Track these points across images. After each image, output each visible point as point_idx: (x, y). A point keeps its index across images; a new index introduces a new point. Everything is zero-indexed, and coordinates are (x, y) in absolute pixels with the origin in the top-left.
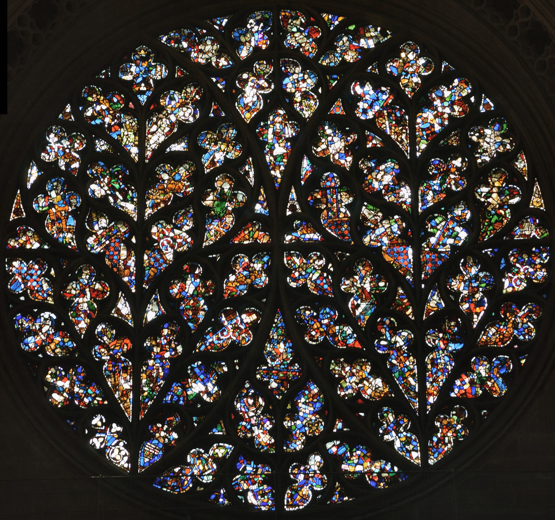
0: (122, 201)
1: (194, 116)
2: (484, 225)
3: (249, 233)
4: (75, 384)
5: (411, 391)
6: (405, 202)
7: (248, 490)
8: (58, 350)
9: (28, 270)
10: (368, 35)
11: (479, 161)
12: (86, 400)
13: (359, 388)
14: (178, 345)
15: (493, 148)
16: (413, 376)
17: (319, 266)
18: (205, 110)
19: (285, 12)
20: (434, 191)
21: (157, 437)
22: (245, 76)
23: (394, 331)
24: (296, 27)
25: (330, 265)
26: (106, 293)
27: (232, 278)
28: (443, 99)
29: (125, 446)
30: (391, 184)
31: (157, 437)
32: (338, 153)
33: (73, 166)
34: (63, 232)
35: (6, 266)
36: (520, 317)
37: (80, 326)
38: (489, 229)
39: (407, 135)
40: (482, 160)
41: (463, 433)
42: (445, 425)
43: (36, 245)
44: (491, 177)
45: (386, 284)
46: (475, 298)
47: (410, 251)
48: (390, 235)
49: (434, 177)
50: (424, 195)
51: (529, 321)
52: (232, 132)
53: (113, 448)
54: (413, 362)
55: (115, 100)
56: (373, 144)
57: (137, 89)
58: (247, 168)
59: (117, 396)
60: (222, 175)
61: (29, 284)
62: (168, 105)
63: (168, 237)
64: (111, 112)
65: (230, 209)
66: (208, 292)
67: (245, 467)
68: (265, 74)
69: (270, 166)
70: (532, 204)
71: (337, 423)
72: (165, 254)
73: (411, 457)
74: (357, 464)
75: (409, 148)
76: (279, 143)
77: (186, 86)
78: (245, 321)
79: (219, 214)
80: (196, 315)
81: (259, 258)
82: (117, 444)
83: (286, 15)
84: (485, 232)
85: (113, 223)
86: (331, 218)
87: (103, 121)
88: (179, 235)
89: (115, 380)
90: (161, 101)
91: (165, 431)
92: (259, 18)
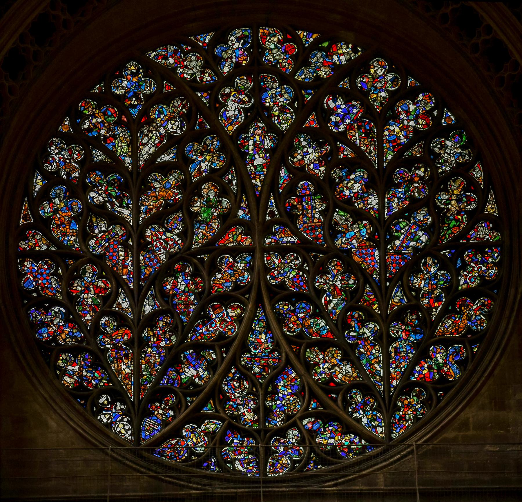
0: (118, 207)
1: (181, 129)
2: (443, 229)
3: (233, 236)
4: (83, 368)
5: (377, 375)
6: (373, 209)
7: (235, 459)
8: (68, 340)
9: (38, 270)
10: (340, 52)
11: (440, 170)
12: (94, 382)
13: (332, 373)
14: (172, 335)
15: (453, 159)
16: (379, 363)
17: (295, 266)
19: (263, 29)
20: (399, 198)
21: (156, 414)
22: (227, 91)
23: (362, 323)
24: (274, 44)
26: (108, 289)
28: (408, 113)
30: (361, 192)
31: (156, 414)
32: (313, 163)
34: (67, 236)
35: (19, 266)
36: (473, 310)
37: (86, 318)
38: (448, 233)
39: (375, 147)
40: (443, 170)
41: (422, 411)
42: (406, 404)
43: (45, 247)
44: (451, 185)
45: (355, 282)
46: (434, 294)
47: (377, 253)
48: (359, 239)
49: (399, 186)
50: (390, 202)
51: (481, 314)
53: (119, 423)
54: (379, 351)
55: (109, 113)
56: (344, 154)
57: (129, 102)
58: (230, 176)
60: (208, 183)
61: (40, 282)
62: (158, 118)
63: (160, 239)
64: (106, 125)
65: (215, 214)
66: (198, 289)
67: (233, 440)
68: (245, 89)
69: (250, 175)
70: (487, 211)
71: (312, 403)
72: (158, 255)
73: (376, 432)
74: (330, 438)
75: (377, 159)
76: (259, 154)
77: (173, 99)
78: (230, 315)
79: (206, 219)
80: (188, 309)
81: (242, 258)
82: (122, 420)
83: (264, 32)
84: (444, 235)
85: (112, 227)
86: (306, 223)
87: (99, 133)
88: (170, 238)
89: (118, 365)
90: (151, 114)
91: (162, 409)
92: (239, 35)
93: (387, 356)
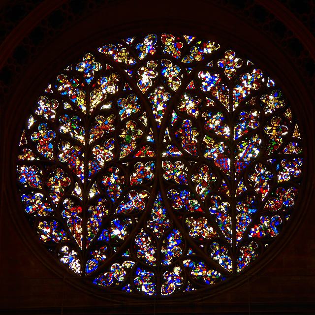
1: (115, 90)
3: (144, 151)
6: (226, 135)
7: (142, 285)
8: (44, 213)
10: (208, 46)
11: (266, 113)
12: (59, 239)
16: (229, 226)
17: (180, 169)
20: (242, 129)
22: (142, 69)
23: (220, 203)
25: (186, 168)
27: (135, 175)
28: (247, 80)
29: (78, 262)
33: (52, 117)
43: (33, 159)
47: (229, 161)
49: (242, 121)
50: (237, 131)
52: (136, 99)
55: (74, 82)
58: (143, 117)
59: (74, 236)
61: (29, 179)
63: (101, 153)
65: (134, 139)
73: (227, 268)
74: (199, 272)
77: (111, 74)
78: (141, 197)
82: (75, 261)
84: (270, 149)
91: (99, 255)
93: (234, 221)
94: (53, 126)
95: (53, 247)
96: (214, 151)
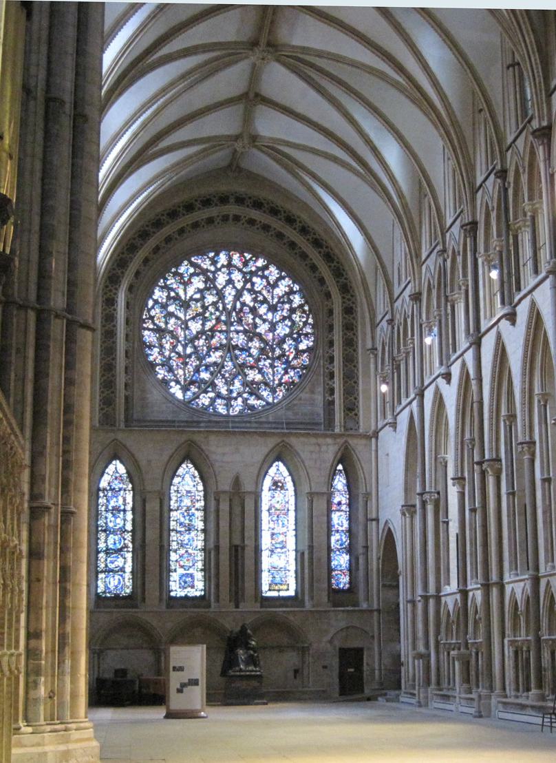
18: (206, 284)
23: (265, 360)
28: (282, 284)
47: (271, 335)
52: (215, 292)
93: (274, 373)
94: (164, 306)
95: (165, 382)
96: (263, 328)
